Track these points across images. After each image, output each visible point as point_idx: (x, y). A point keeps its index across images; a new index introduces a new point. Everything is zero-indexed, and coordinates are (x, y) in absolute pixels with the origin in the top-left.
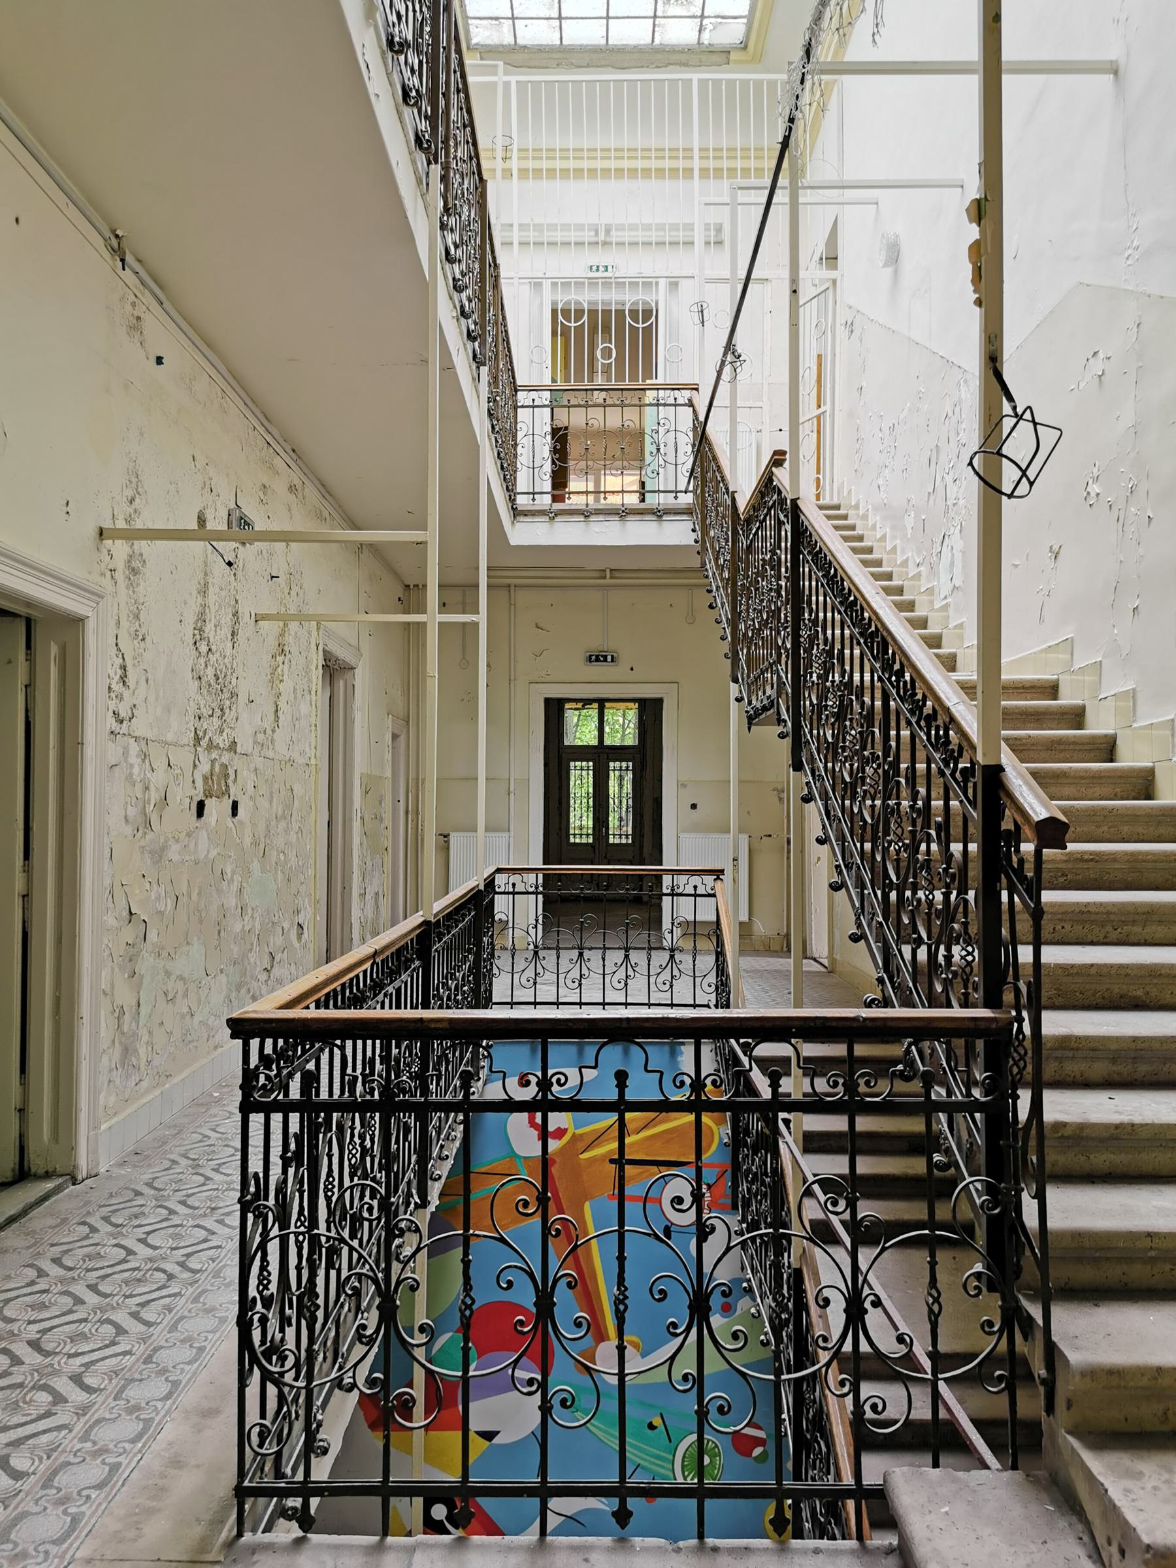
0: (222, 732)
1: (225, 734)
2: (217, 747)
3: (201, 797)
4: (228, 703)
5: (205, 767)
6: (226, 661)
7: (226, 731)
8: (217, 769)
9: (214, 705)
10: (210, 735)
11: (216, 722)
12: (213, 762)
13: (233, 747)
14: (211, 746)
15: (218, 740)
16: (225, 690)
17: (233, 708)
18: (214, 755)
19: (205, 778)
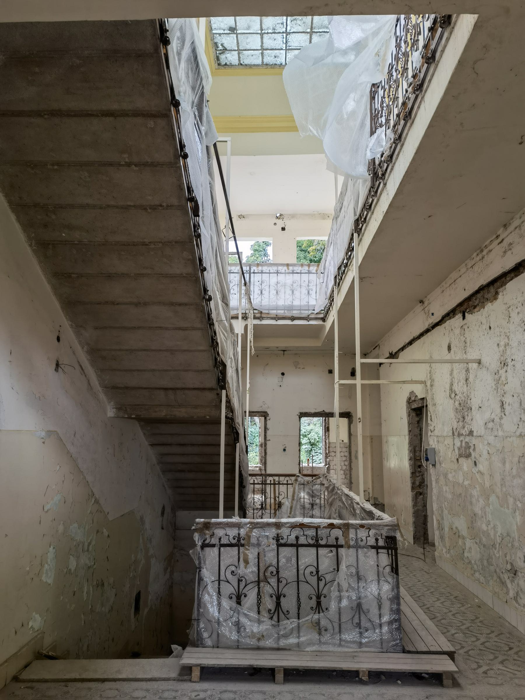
0: (464, 427)
1: (466, 429)
2: (462, 435)
3: (457, 457)
4: (466, 413)
5: (458, 444)
6: (464, 394)
7: (466, 427)
8: (464, 444)
9: (460, 417)
10: (459, 430)
11: (461, 424)
12: (461, 441)
13: (471, 433)
14: (459, 435)
15: (463, 432)
16: (464, 408)
17: (470, 415)
18: (462, 438)
19: (459, 449)
